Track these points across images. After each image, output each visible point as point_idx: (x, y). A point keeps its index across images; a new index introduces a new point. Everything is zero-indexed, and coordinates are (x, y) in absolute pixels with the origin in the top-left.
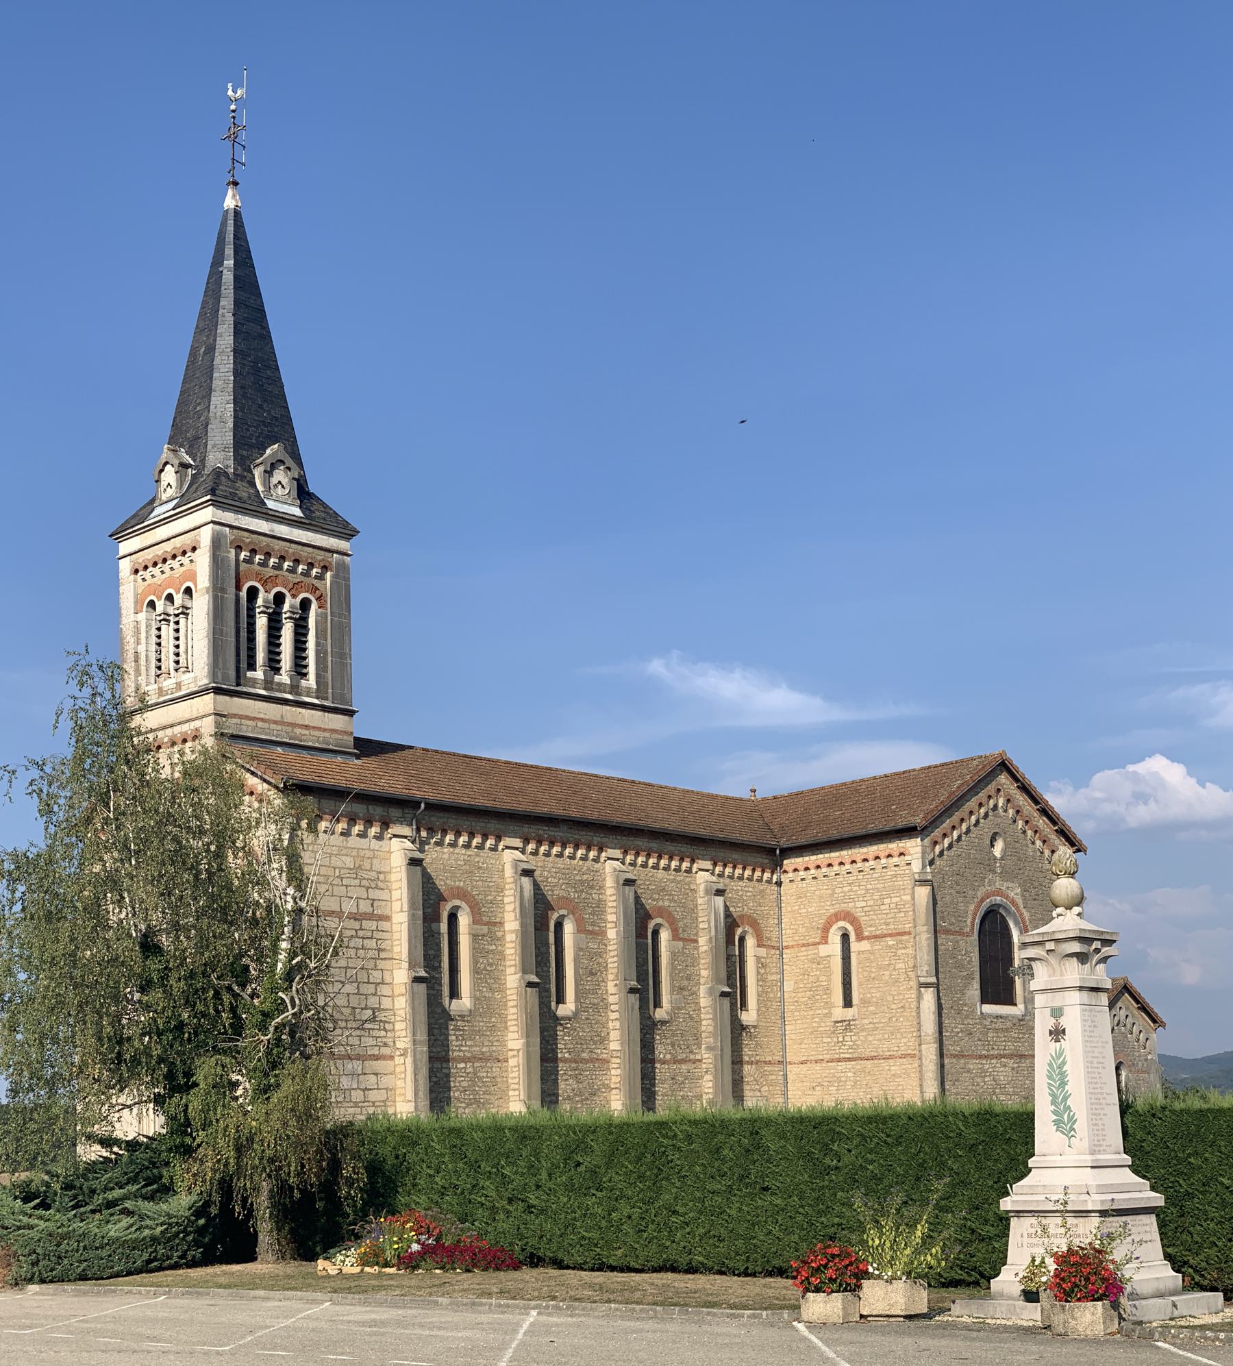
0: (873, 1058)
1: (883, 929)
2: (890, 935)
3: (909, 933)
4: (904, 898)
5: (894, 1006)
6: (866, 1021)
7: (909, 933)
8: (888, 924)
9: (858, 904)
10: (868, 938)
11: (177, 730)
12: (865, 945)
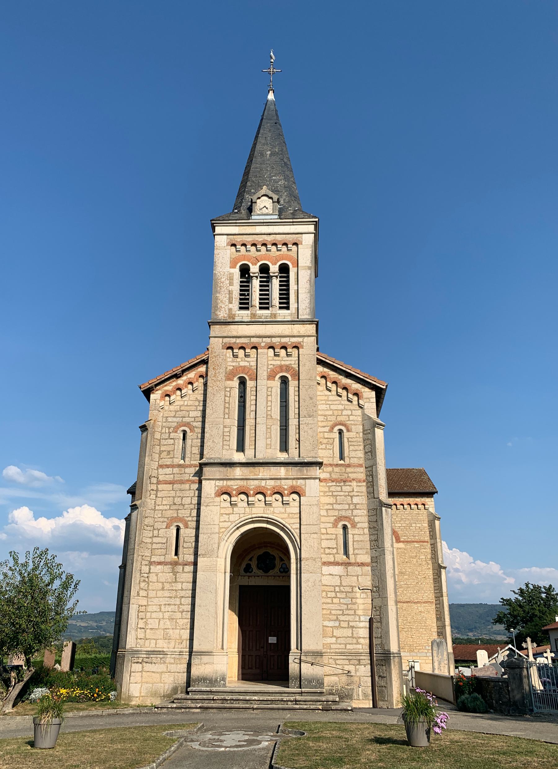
0: (407, 602)
1: (412, 538)
2: (417, 542)
3: (427, 542)
4: (424, 525)
5: (419, 577)
6: (402, 583)
7: (427, 542)
8: (415, 536)
9: (396, 525)
10: (403, 542)
11: (274, 340)
12: (401, 545)
